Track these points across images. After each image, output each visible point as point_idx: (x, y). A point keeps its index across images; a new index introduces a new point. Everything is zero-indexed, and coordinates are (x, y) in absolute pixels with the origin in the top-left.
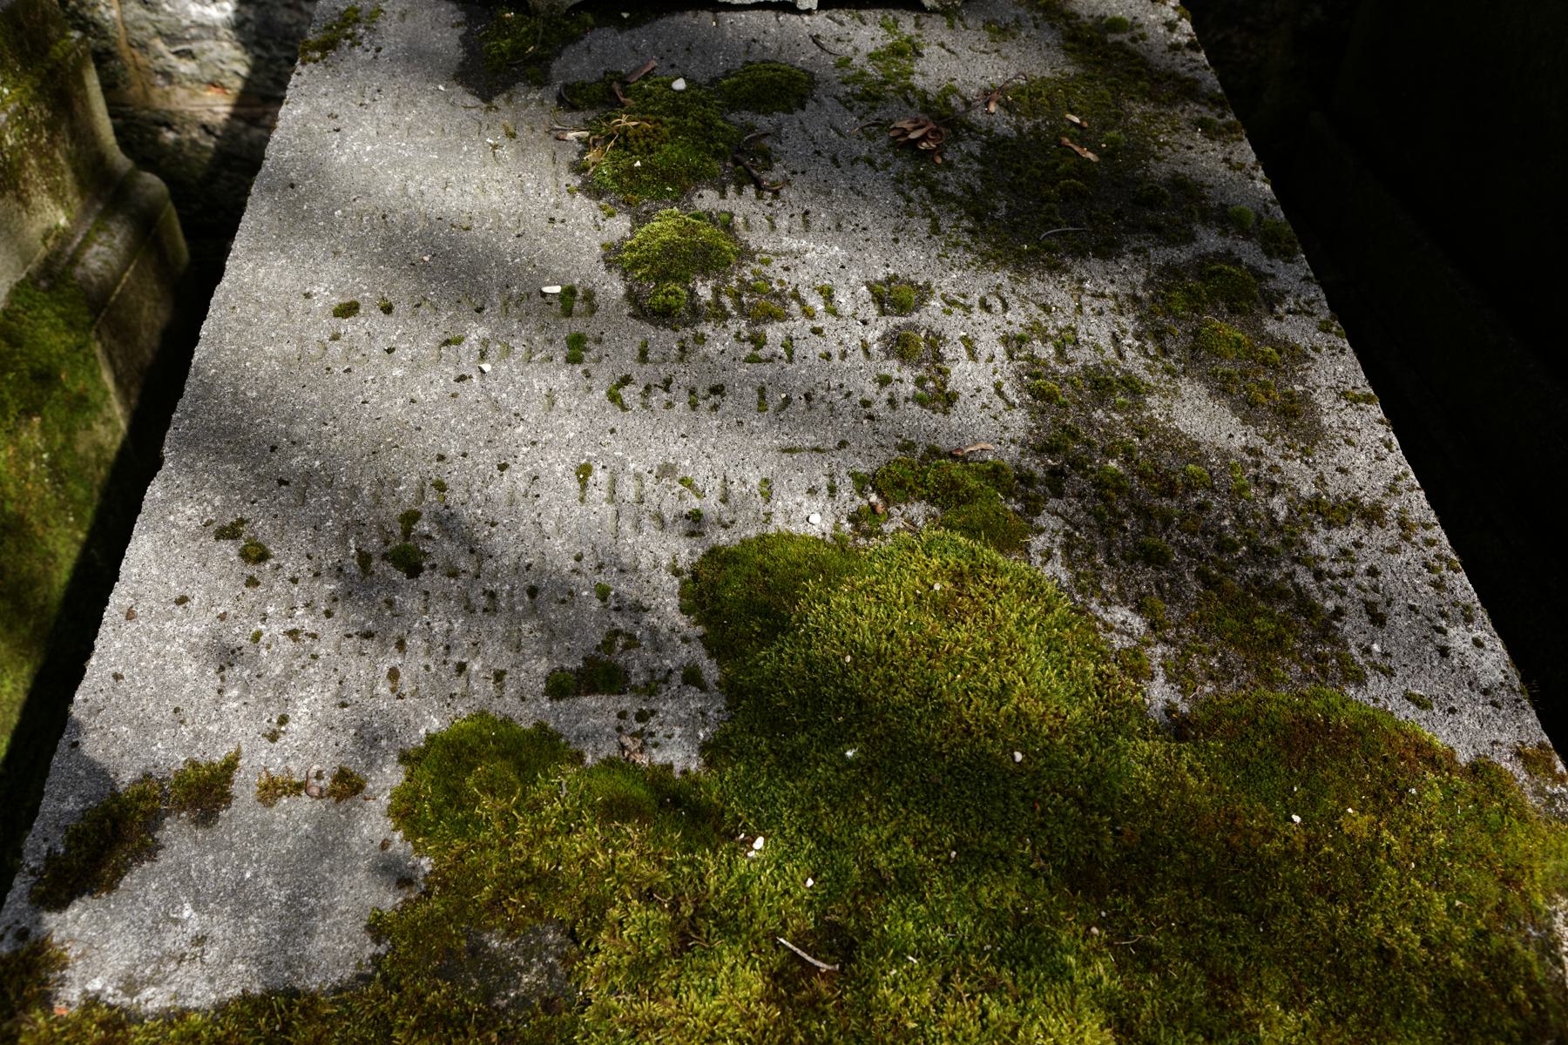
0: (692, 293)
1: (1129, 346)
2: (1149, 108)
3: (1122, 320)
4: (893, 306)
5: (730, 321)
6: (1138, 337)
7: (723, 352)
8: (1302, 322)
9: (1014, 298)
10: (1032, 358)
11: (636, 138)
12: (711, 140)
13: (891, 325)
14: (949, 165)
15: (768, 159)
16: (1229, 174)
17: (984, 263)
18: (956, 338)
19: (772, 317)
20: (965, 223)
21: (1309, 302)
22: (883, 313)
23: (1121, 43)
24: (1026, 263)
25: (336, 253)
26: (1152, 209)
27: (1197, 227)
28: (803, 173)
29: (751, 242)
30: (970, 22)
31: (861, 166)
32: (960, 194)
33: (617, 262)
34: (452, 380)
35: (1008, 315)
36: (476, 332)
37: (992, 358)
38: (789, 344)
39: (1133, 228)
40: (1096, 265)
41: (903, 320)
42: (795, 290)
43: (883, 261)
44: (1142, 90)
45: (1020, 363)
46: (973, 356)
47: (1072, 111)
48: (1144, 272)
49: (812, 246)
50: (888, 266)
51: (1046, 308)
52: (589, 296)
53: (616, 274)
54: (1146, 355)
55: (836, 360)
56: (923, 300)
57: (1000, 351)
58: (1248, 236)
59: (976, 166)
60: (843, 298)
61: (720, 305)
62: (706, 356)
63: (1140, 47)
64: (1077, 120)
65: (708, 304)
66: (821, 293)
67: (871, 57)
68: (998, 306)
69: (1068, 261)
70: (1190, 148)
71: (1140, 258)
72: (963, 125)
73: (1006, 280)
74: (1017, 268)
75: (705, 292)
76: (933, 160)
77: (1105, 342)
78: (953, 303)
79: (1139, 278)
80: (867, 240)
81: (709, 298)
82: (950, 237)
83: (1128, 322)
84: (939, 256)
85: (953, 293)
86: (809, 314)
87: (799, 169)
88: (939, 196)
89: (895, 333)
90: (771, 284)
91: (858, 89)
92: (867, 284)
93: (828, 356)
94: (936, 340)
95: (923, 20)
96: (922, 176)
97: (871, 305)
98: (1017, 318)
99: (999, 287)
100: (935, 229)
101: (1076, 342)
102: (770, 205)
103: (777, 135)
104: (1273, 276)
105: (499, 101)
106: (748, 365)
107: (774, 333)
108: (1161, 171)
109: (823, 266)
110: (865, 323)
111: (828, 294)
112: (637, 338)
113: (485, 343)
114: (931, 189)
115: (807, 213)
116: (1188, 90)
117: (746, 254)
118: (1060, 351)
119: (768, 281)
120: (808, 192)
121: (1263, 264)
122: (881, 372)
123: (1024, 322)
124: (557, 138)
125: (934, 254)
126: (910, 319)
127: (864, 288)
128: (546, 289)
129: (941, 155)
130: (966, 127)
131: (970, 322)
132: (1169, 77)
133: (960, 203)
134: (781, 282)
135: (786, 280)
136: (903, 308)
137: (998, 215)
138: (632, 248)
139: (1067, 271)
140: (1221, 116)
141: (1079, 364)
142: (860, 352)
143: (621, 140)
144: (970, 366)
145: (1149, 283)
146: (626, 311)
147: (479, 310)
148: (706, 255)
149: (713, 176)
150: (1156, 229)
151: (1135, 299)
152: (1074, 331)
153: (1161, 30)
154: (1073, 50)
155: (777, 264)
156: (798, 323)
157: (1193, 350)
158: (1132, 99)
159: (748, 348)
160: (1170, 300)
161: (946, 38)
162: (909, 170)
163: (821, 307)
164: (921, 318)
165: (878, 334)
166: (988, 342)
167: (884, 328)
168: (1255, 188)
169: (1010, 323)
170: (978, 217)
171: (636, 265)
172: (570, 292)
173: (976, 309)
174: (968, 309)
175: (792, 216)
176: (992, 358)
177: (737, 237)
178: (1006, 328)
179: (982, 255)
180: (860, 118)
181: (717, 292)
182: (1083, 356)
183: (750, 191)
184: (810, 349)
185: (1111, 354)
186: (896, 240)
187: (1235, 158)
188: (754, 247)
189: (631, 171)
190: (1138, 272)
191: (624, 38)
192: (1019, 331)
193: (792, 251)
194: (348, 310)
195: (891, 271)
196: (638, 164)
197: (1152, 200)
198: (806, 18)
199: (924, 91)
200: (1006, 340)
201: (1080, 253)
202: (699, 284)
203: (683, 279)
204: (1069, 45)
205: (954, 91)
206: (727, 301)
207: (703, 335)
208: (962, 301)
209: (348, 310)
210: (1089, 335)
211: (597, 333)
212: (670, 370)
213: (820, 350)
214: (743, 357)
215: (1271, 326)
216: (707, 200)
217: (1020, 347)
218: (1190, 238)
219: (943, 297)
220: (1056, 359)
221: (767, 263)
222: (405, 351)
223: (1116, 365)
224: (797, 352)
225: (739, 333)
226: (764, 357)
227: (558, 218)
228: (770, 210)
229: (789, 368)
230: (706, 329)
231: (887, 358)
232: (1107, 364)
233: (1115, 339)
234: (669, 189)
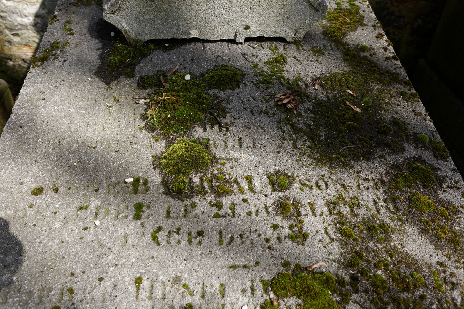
0: (191, 180)
1: (382, 206)
2: (380, 86)
3: (378, 192)
4: (278, 186)
5: (207, 195)
6: (385, 201)
7: (203, 212)
8: (455, 193)
9: (330, 181)
10: (339, 213)
11: (169, 104)
12: (201, 103)
13: (277, 197)
14: (299, 114)
15: (224, 112)
16: (416, 117)
17: (316, 163)
18: (306, 203)
19: (226, 193)
20: (308, 143)
21: (457, 182)
22: (274, 190)
23: (365, 57)
24: (334, 163)
25: (36, 161)
26: (385, 135)
27: (405, 144)
28: (239, 119)
29: (216, 154)
30: (305, 47)
31: (263, 115)
32: (305, 128)
33: (158, 164)
34: (81, 229)
35: (328, 190)
36: (95, 203)
37: (322, 214)
38: (233, 207)
39: (378, 145)
40: (364, 164)
41: (283, 194)
42: (236, 178)
43: (273, 163)
44: (376, 78)
45: (335, 216)
46: (314, 214)
47: (349, 88)
48: (385, 167)
49: (243, 155)
50: (275, 165)
51: (344, 187)
52: (146, 182)
53: (158, 171)
54: (389, 211)
55: (254, 215)
56: (291, 183)
57: (326, 210)
58: (427, 149)
59: (311, 115)
60: (256, 183)
61: (202, 187)
62: (196, 214)
63: (373, 58)
64: (351, 92)
65: (198, 186)
66: (247, 180)
67: (266, 63)
68: (324, 186)
69: (352, 162)
70: (398, 105)
71: (383, 160)
72: (305, 95)
73: (326, 172)
74: (331, 167)
75: (196, 180)
76: (293, 112)
77: (371, 204)
78: (304, 184)
79: (383, 170)
80: (266, 152)
81: (198, 183)
82: (301, 150)
83: (380, 194)
84: (297, 160)
85: (303, 178)
86: (242, 191)
87: (237, 117)
88: (296, 130)
89: (279, 201)
90: (225, 175)
91: (261, 78)
92: (267, 175)
93: (250, 214)
94: (297, 204)
95: (287, 46)
96: (288, 120)
97: (269, 186)
98: (332, 192)
99: (323, 176)
100: (295, 146)
101: (358, 205)
102: (225, 135)
103: (228, 100)
104: (439, 169)
105: (113, 85)
106: (214, 219)
107: (226, 201)
108: (387, 116)
109: (248, 166)
110: (266, 196)
111: (250, 180)
112: (166, 205)
113: (98, 208)
114: (293, 126)
115: (240, 139)
116: (395, 78)
117: (215, 160)
118: (352, 210)
119: (223, 174)
120: (241, 129)
121: (434, 162)
122: (274, 223)
123: (335, 194)
124: (136, 103)
125: (295, 160)
126: (286, 193)
127: (265, 177)
128: (126, 180)
129: (296, 110)
130: (306, 96)
131: (312, 195)
132: (387, 72)
133: (305, 133)
134: (229, 174)
135: (232, 173)
136: (282, 188)
137: (321, 139)
138: (165, 158)
139: (352, 167)
140: (410, 90)
141: (360, 216)
142: (264, 211)
143: (163, 105)
144: (313, 218)
145: (387, 173)
146: (161, 191)
147: (96, 191)
148: (197, 161)
149: (201, 121)
150: (388, 146)
151: (382, 182)
152: (357, 199)
153: (382, 51)
154: (347, 60)
155: (228, 165)
156: (237, 196)
157: (409, 208)
158: (373, 82)
159: (215, 210)
160: (398, 182)
161: (296, 54)
162: (283, 117)
163: (247, 187)
164: (290, 193)
165: (272, 201)
166: (321, 207)
167: (274, 199)
168: (427, 124)
169: (329, 195)
170: (313, 139)
171: (166, 166)
172: (137, 181)
173: (314, 187)
174: (310, 187)
175: (234, 140)
176: (322, 214)
177: (210, 151)
178: (327, 197)
179: (315, 159)
180: (262, 92)
181: (201, 179)
182: (362, 212)
183: (216, 128)
184: (242, 210)
185: (374, 211)
186: (279, 152)
187: (417, 110)
188: (218, 156)
189: (167, 119)
190: (382, 167)
191: (166, 55)
192: (332, 199)
193: (234, 158)
194: (38, 192)
195: (277, 168)
196: (169, 116)
197: (384, 131)
198: (240, 46)
199: (288, 79)
200: (328, 204)
201: (357, 158)
202: (194, 176)
203: (187, 174)
204: (346, 58)
205: (300, 79)
206: (205, 184)
207: (195, 203)
208: (308, 183)
209: (38, 192)
210: (364, 201)
211: (148, 203)
212: (180, 223)
213: (247, 211)
214: (212, 215)
215: (442, 195)
216: (198, 132)
217: (334, 208)
218: (403, 150)
219: (300, 181)
220: (350, 214)
221: (223, 164)
222: (62, 214)
223: (376, 217)
224: (236, 212)
225: (211, 202)
226: (222, 215)
227: (134, 142)
228: (225, 137)
229: (233, 220)
230: (196, 200)
231: (276, 215)
232: (372, 216)
233: (375, 203)
234: (182, 128)
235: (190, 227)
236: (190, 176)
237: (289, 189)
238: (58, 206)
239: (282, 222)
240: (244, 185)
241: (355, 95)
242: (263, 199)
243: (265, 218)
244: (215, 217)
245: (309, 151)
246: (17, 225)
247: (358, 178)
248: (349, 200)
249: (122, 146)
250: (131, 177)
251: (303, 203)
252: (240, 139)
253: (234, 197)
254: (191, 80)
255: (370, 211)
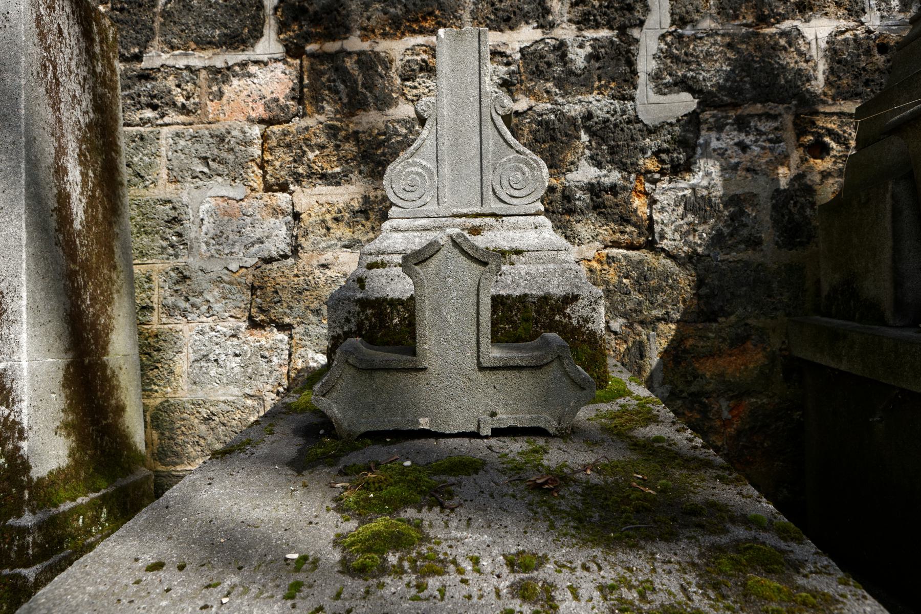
0: (385, 560)
1: (694, 592)
2: (685, 472)
3: (686, 576)
4: (520, 567)
5: (405, 575)
6: (700, 586)
7: (394, 593)
8: (825, 579)
9: (606, 563)
10: (621, 599)
11: (374, 483)
12: (419, 486)
13: (517, 577)
14: (563, 497)
15: (451, 495)
16: (743, 500)
17: (584, 544)
18: (564, 586)
19: (434, 573)
20: (572, 524)
21: (825, 567)
22: (513, 571)
23: (662, 446)
24: (613, 544)
25: (170, 538)
26: (695, 516)
27: (729, 525)
28: (471, 501)
29: (431, 533)
30: (576, 440)
31: (507, 498)
32: (568, 510)
33: (341, 543)
34: (198, 609)
35: (602, 573)
36: (232, 579)
37: (591, 599)
38: (442, 591)
39: (686, 526)
40: (662, 545)
41: (527, 575)
42: (455, 558)
43: (516, 543)
44: (678, 464)
45: (612, 602)
46: (576, 597)
47: (637, 473)
48: (696, 549)
49: (470, 535)
50: (519, 545)
51: (629, 569)
52: (316, 561)
53: (339, 549)
54: (709, 598)
55: (475, 599)
56: (541, 564)
57: (596, 594)
58: (765, 530)
59: (579, 497)
60: (485, 563)
61: (401, 566)
62: (382, 596)
63: (674, 448)
64: (641, 477)
65: (394, 566)
66: (471, 560)
67: (519, 453)
68: (595, 567)
69: (643, 543)
70: (714, 488)
71: (693, 541)
72: (571, 480)
73: (600, 553)
74: (607, 546)
75: (393, 559)
76: (552, 495)
77: (675, 589)
78: (564, 566)
79: (695, 552)
80: (507, 532)
81: (395, 563)
82: (562, 530)
83: (691, 577)
84: (554, 540)
85: (563, 560)
86: (460, 571)
87: (469, 499)
88: (555, 511)
89: (519, 583)
90: (438, 555)
91: (510, 466)
92: (504, 555)
93: (470, 597)
94: (549, 587)
95: (550, 440)
96: (545, 501)
97: (505, 566)
98: (609, 575)
99: (595, 557)
100: (552, 526)
101: (654, 589)
102: (448, 515)
103: (459, 484)
104: (792, 551)
105: (306, 473)
106: (410, 602)
107: (433, 583)
108: (698, 499)
109: (475, 545)
110: (498, 576)
111: (476, 561)
112: (338, 585)
113: (233, 587)
114: (550, 508)
115: (470, 519)
116: (707, 464)
117: (426, 539)
118: (642, 596)
119: (437, 553)
120: (472, 510)
121: (782, 545)
122: (507, 607)
123: (614, 577)
124: (331, 487)
125: (550, 539)
126: (532, 575)
127: (502, 557)
128: (289, 556)
129: (557, 492)
130: (573, 481)
131: (574, 577)
132: (694, 459)
133: (568, 514)
134: (446, 554)
135: (449, 553)
136: (526, 568)
137: (593, 520)
138: (353, 536)
139: (643, 548)
140: (730, 474)
141: (657, 603)
142: (494, 595)
143: (365, 486)
144: (574, 603)
145: (701, 555)
146: (336, 569)
147: (240, 568)
148: (399, 538)
149: (416, 502)
150: (701, 526)
151: (693, 564)
152: (652, 583)
153: (685, 442)
154: (635, 450)
155: (444, 545)
156: (451, 577)
157: (745, 596)
158: (674, 468)
159: (413, 591)
160: (719, 564)
161: (563, 446)
162: (537, 499)
163: (470, 568)
164: (539, 574)
165: (507, 583)
166: (587, 588)
167: (512, 580)
168: (762, 506)
169: (603, 577)
170: (580, 521)
171: (352, 544)
172: (304, 558)
173: (579, 569)
174: (573, 570)
175: (460, 520)
176: (591, 599)
177: (422, 531)
178: (600, 580)
179: (583, 540)
180: (510, 477)
181: (401, 559)
182: (659, 599)
183: (437, 509)
184: (457, 592)
185: (681, 597)
186: (526, 532)
187: (745, 492)
188: (432, 535)
189: (367, 499)
190: (693, 549)
191: (384, 449)
192: (610, 582)
193: (456, 538)
194: (157, 566)
195: (521, 548)
196: (372, 495)
197: (695, 511)
198: (486, 440)
199: (549, 466)
200: (601, 588)
201: (650, 538)
202: (391, 554)
203: (381, 552)
204: (632, 447)
205: (566, 466)
206: (406, 564)
207: (384, 583)
208: (569, 565)
209: (157, 566)
210: (663, 585)
211: (311, 581)
212: (353, 604)
213: (464, 593)
214: (408, 597)
215: (801, 581)
216: (411, 513)
217: (612, 592)
218: (726, 531)
219: (556, 563)
220: (640, 601)
221: (439, 544)
222: (178, 591)
223: (686, 604)
224: (447, 594)
225: (410, 582)
226: (423, 597)
227: (314, 522)
228: (447, 518)
229: (440, 604)
230: (387, 580)
231: (513, 598)
232: (679, 604)
233: (683, 589)
234: (387, 507)
235: (368, 610)
236: (385, 556)
237: (537, 570)
238: (176, 583)
239: (521, 606)
240: (468, 566)
241: (646, 478)
242: (494, 581)
243: (493, 602)
244: (413, 600)
245: (573, 532)
246: (106, 601)
247: (653, 561)
248: (638, 583)
249: (296, 525)
250: (296, 553)
251: (558, 586)
252: (470, 519)
253: (446, 577)
254: (411, 466)
255: (674, 597)
